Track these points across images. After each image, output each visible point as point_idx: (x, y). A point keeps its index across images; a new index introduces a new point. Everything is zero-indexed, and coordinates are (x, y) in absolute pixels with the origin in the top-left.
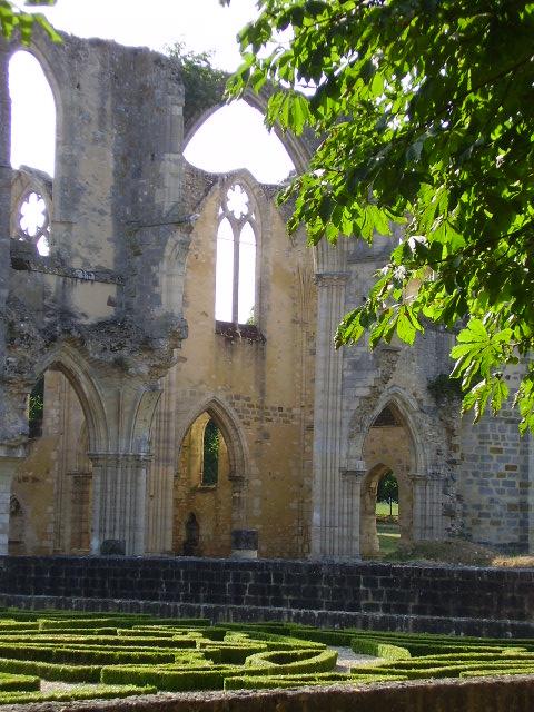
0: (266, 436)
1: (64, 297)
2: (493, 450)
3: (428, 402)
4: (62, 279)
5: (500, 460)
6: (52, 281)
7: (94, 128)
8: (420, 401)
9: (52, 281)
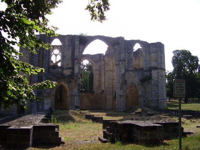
0: (132, 90)
1: (62, 72)
2: (153, 90)
3: (140, 83)
5: (155, 92)
6: (60, 70)
7: (67, 47)
8: (138, 83)
9: (60, 70)
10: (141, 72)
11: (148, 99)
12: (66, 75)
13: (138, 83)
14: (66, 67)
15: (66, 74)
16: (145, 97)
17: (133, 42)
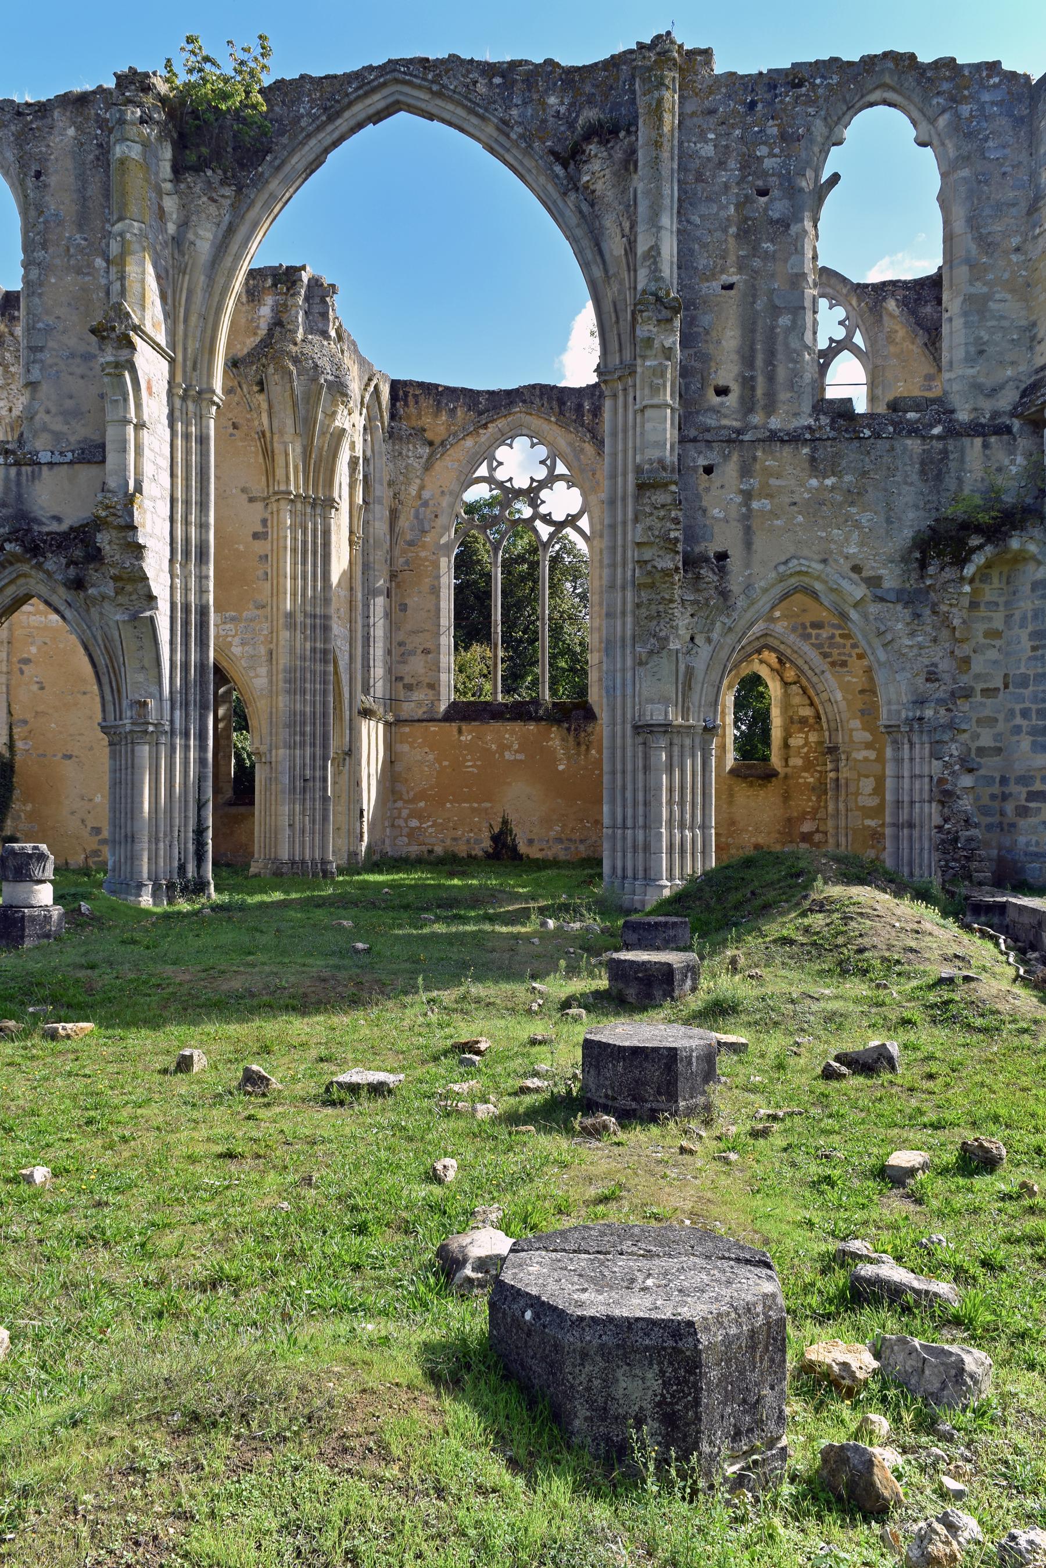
4: (13, 471)
8: (873, 582)
10: (913, 445)
11: (990, 766)
12: (55, 527)
13: (873, 582)
14: (57, 436)
15: (58, 519)
16: (954, 749)
17: (825, 92)
